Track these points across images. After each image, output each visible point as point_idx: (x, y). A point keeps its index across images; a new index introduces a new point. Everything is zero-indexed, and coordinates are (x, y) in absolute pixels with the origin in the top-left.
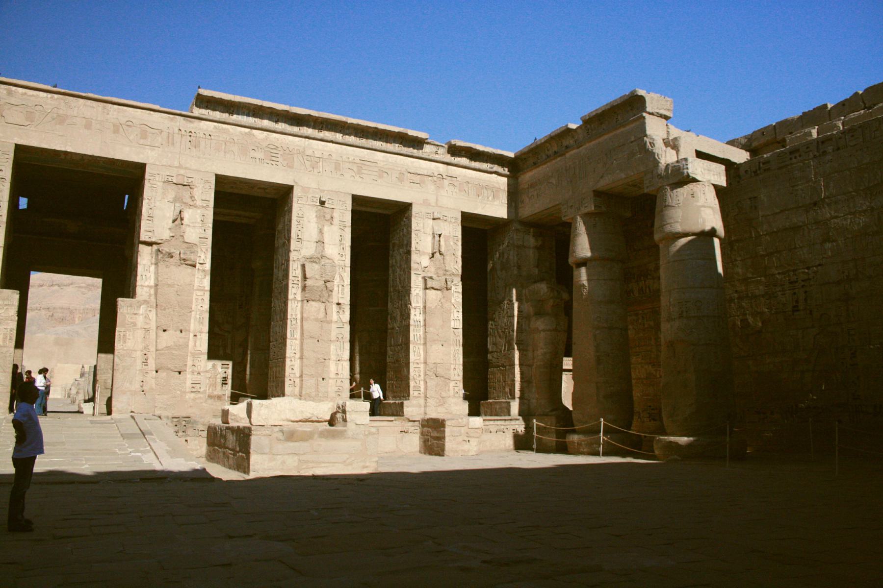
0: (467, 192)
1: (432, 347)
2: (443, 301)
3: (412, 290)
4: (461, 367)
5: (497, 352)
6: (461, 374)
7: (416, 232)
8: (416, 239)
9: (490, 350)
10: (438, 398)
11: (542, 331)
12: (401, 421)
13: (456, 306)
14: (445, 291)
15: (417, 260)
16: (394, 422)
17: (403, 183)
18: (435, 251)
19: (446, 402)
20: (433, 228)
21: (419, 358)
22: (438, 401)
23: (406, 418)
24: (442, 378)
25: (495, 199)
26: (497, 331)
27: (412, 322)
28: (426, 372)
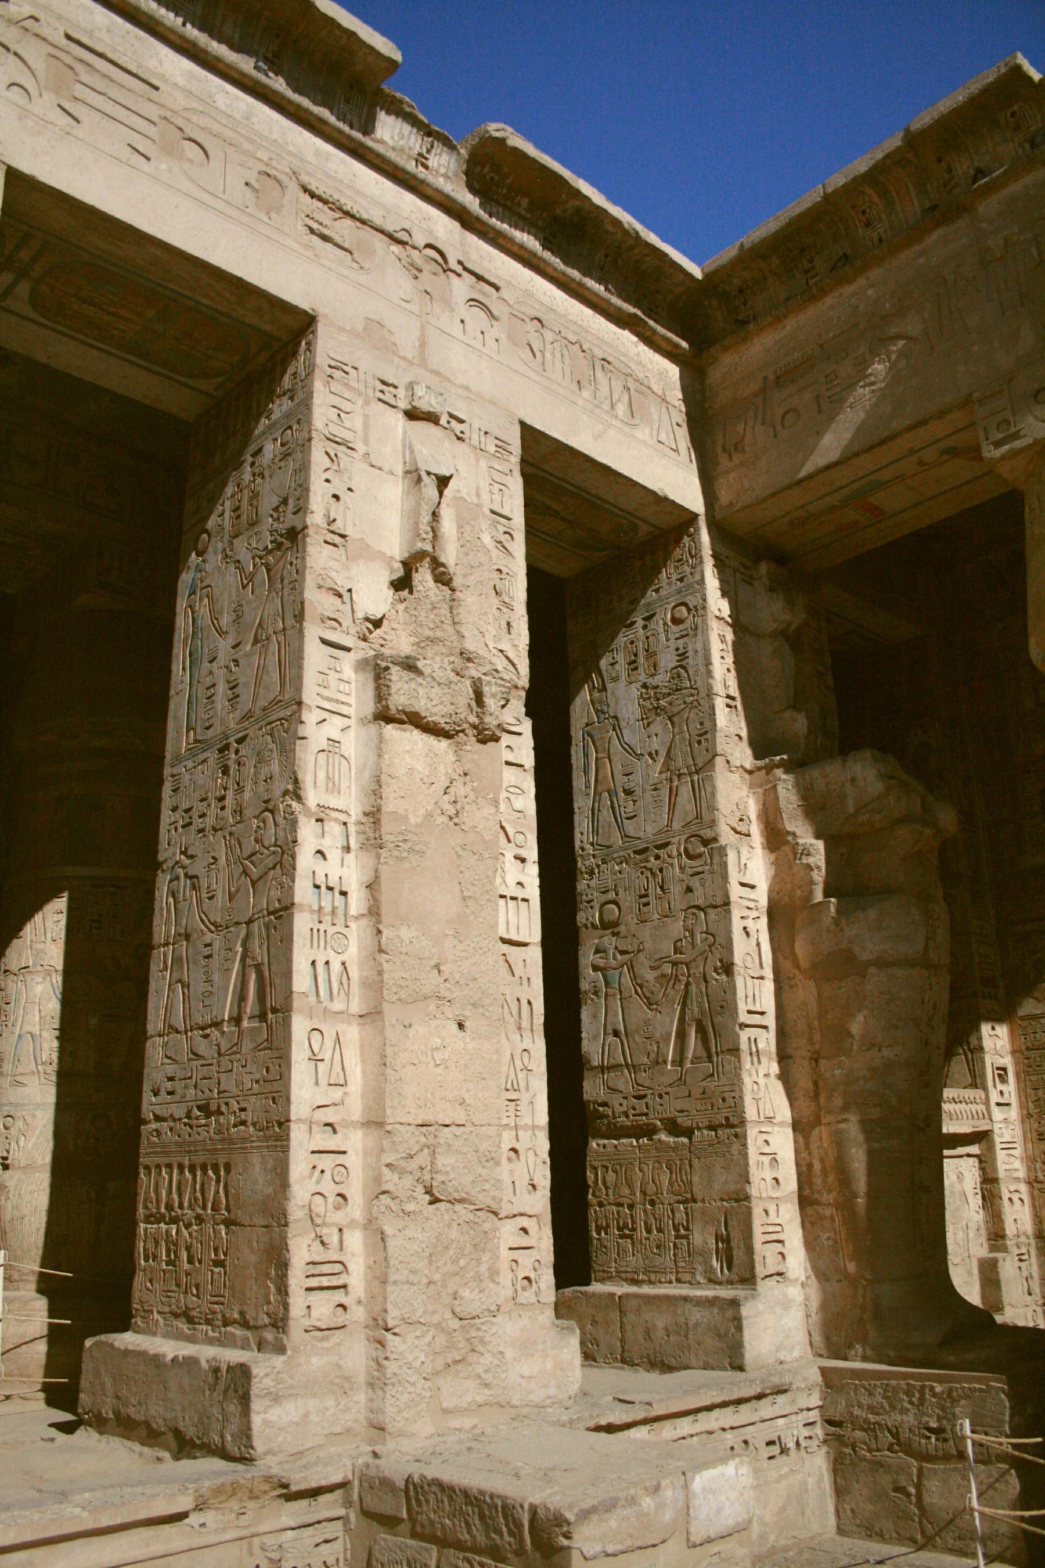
0: (538, 354)
1: (411, 1032)
2: (460, 789)
3: (310, 717)
4: (544, 1145)
5: (634, 1068)
6: (544, 1177)
7: (332, 448)
8: (327, 475)
9: (596, 1062)
10: (438, 1326)
11: (870, 963)
12: (234, 1505)
13: (511, 832)
14: (471, 745)
15: (334, 574)
16: (194, 1519)
17: (273, 215)
18: (420, 545)
19: (482, 1341)
20: (409, 447)
21: (337, 1094)
22: (441, 1340)
23: (267, 1479)
24: (458, 1207)
25: (637, 420)
26: (634, 977)
27: (303, 892)
28: (378, 1180)
